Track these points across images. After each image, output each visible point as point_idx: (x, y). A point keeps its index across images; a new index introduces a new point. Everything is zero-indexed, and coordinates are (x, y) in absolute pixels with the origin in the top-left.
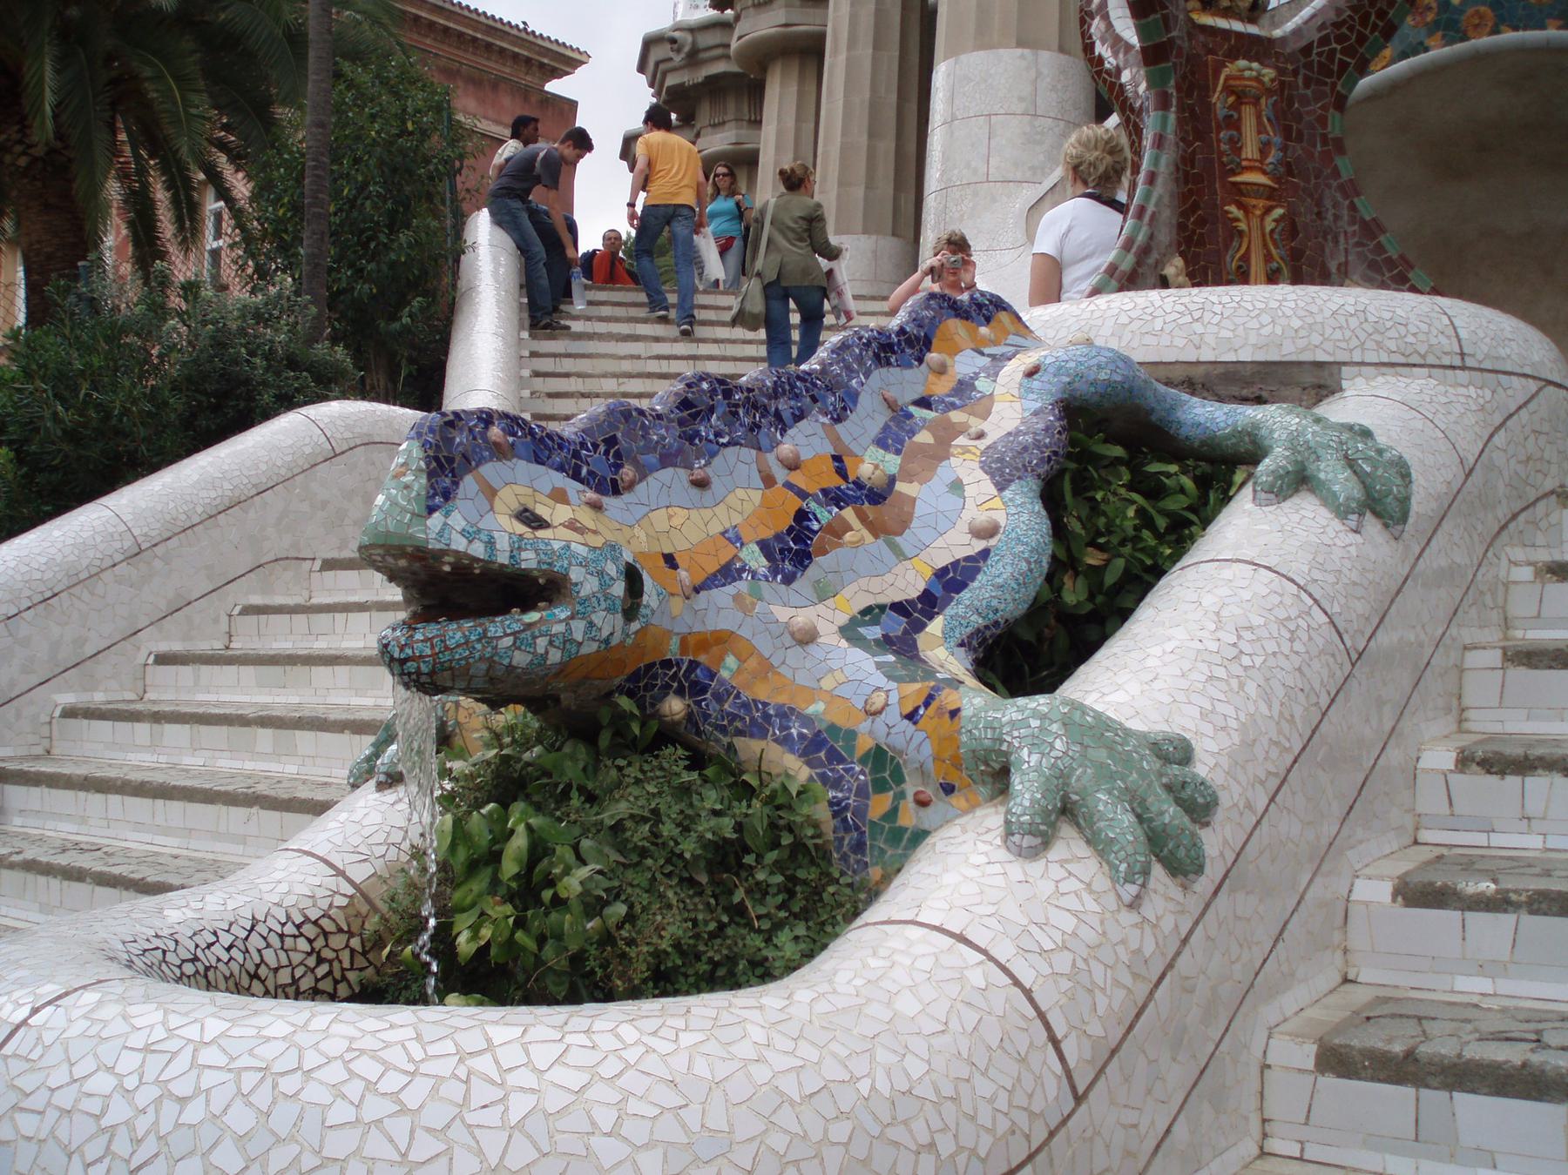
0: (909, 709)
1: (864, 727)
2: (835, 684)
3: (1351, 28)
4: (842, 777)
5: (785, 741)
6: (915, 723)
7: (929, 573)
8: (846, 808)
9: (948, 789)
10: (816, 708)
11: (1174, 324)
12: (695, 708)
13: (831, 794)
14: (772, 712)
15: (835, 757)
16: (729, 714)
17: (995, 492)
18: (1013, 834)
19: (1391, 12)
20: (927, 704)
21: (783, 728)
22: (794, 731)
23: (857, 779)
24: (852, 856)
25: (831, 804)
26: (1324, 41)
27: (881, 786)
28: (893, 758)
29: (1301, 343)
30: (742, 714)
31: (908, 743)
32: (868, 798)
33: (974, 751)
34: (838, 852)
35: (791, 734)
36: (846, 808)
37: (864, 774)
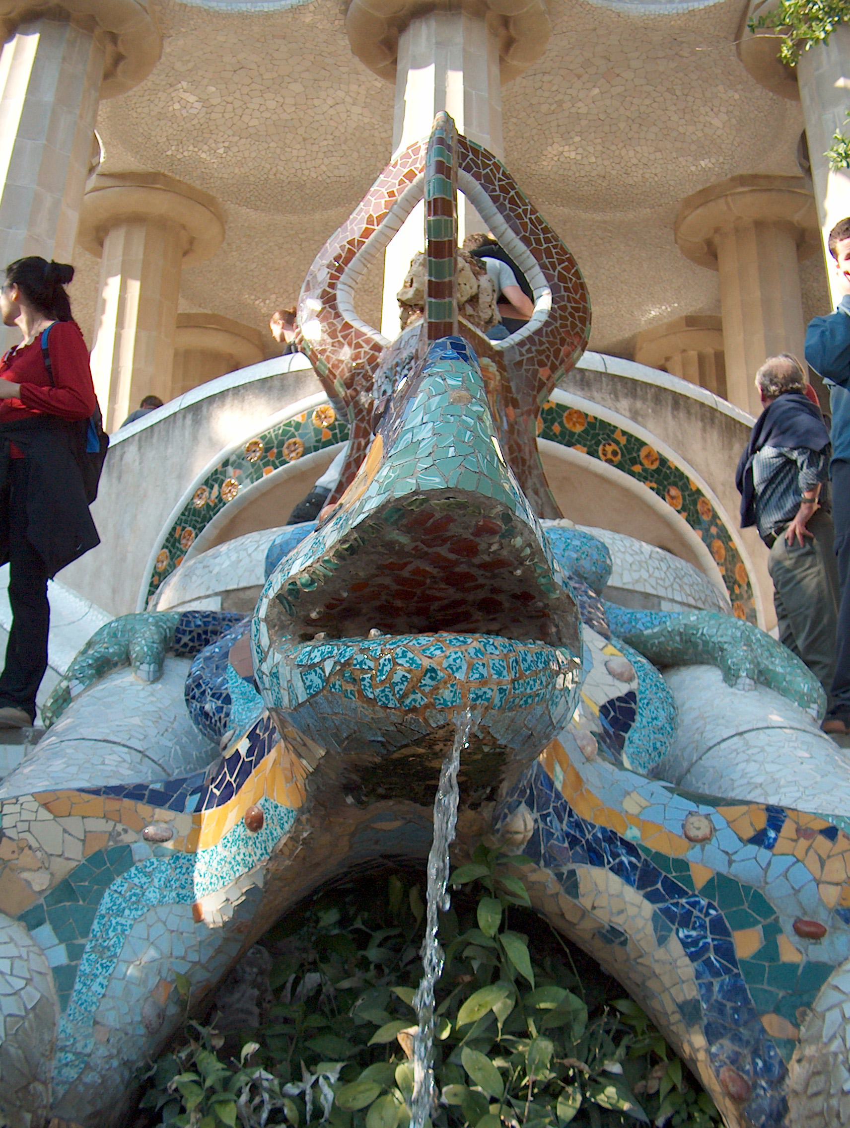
0: (750, 833)
1: (692, 855)
2: (639, 809)
3: (548, 357)
5: (619, 870)
6: (770, 847)
7: (596, 711)
8: (706, 947)
10: (631, 834)
12: (541, 825)
14: (600, 835)
15: (673, 889)
16: (568, 835)
17: (606, 641)
20: (778, 829)
21: (615, 855)
22: (625, 859)
23: (707, 914)
24: (729, 1005)
25: (685, 944)
27: (745, 923)
28: (747, 888)
29: (636, 576)
30: (578, 835)
31: (766, 870)
32: (729, 935)
34: (707, 1001)
36: (706, 947)
37: (714, 908)
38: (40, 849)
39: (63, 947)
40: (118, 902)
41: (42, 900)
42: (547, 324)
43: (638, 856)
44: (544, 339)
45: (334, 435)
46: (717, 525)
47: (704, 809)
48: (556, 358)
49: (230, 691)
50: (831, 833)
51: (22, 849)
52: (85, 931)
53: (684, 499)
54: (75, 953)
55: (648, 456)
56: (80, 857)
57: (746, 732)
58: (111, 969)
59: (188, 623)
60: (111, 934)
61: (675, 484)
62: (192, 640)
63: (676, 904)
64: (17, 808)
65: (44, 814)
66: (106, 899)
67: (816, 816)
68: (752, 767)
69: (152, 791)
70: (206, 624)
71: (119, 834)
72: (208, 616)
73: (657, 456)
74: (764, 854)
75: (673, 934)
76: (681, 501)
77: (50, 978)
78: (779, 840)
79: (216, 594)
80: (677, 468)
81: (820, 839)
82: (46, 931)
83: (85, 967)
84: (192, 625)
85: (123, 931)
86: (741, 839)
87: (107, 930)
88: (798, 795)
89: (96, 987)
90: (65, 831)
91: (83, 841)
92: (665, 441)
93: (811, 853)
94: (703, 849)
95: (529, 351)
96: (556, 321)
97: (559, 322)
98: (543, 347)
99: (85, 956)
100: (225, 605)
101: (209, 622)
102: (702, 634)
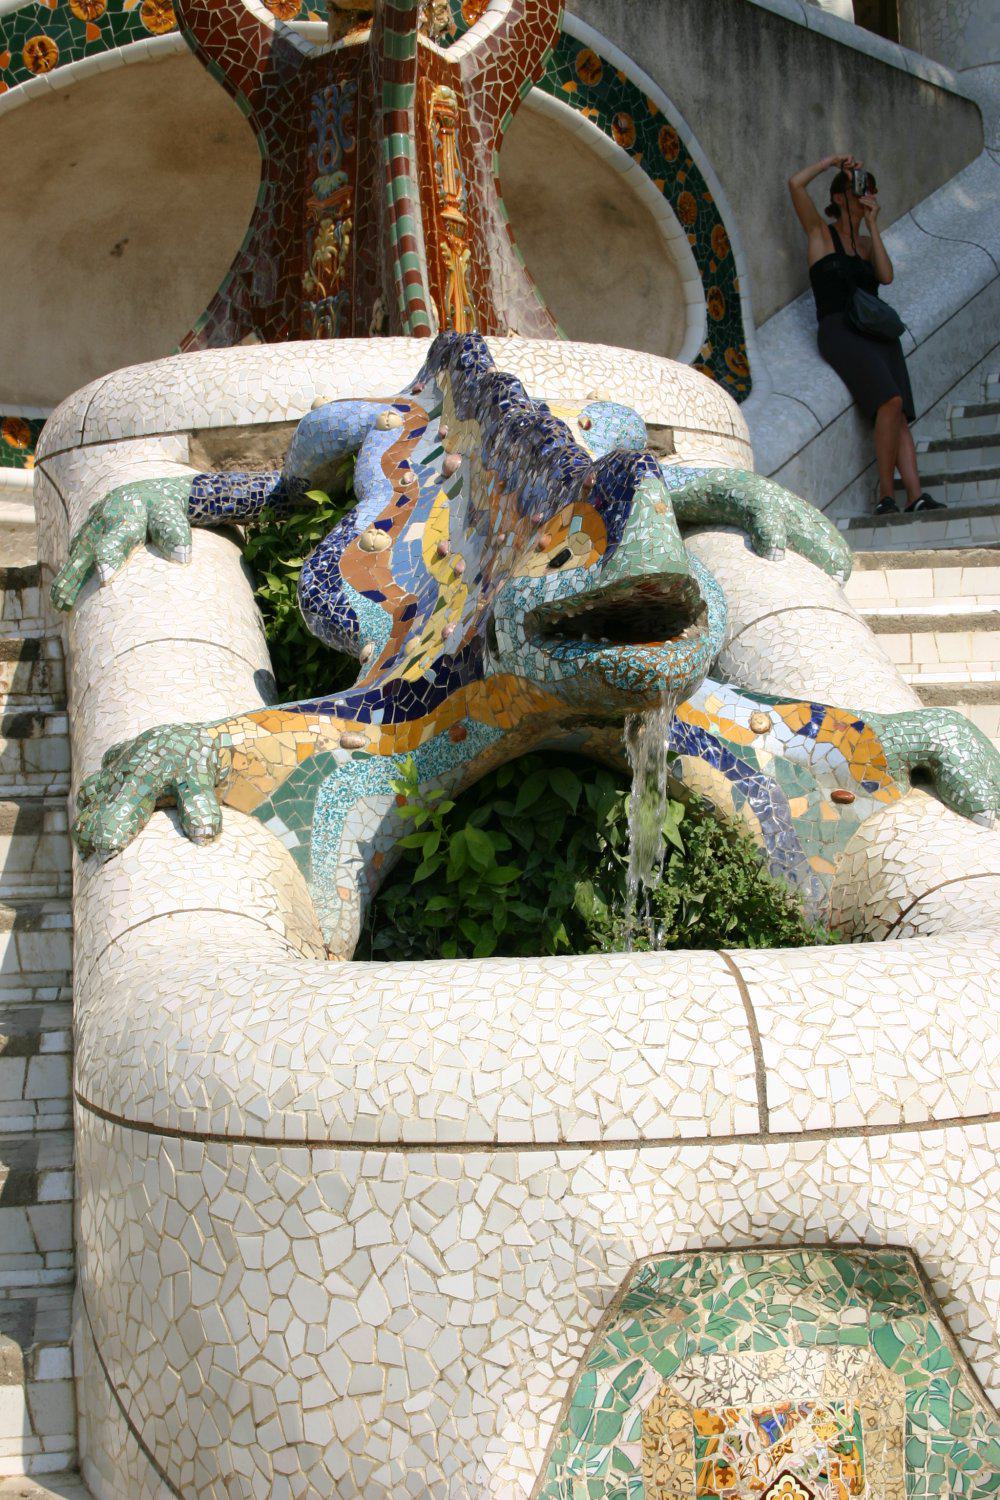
0: (799, 726)
3: (512, 65)
4: (757, 787)
5: (708, 757)
6: (814, 737)
9: (872, 787)
11: (543, 377)
13: (753, 801)
16: (675, 735)
18: (983, 811)
19: (542, 55)
20: (819, 723)
21: (704, 747)
25: (755, 809)
26: (491, 75)
30: (681, 734)
31: (811, 754)
33: (899, 754)
35: (709, 753)
38: (264, 759)
39: (293, 832)
40: (331, 796)
41: (269, 799)
42: (510, 17)
43: (719, 747)
44: (508, 41)
45: (106, 34)
46: (685, 169)
47: (765, 708)
48: (522, 64)
49: (352, 606)
50: (859, 726)
51: (250, 761)
52: (309, 820)
53: (639, 132)
54: (304, 837)
55: (584, 67)
56: (295, 763)
57: (781, 611)
58: (337, 848)
59: (201, 490)
60: (331, 821)
61: (625, 108)
62: (205, 510)
63: (748, 781)
64: (239, 728)
65: (262, 732)
66: (321, 795)
67: (850, 712)
68: (788, 650)
69: (338, 707)
70: (218, 490)
71: (322, 744)
72: (216, 482)
73: (598, 64)
74: (810, 742)
75: (746, 803)
76: (634, 136)
77: (290, 857)
78: (821, 731)
79: (180, 432)
80: (629, 84)
81: (852, 729)
82: (276, 822)
83: (315, 847)
84: (205, 493)
85: (340, 818)
86: (792, 731)
87: (327, 819)
88: (830, 680)
89: (328, 860)
90: (281, 744)
91: (296, 751)
92: (612, 38)
93: (845, 741)
94: (765, 739)
95: (490, 60)
96: (522, 13)
97: (526, 12)
98: (507, 52)
99: (313, 839)
100: (193, 445)
101: (220, 488)
102: (730, 497)
